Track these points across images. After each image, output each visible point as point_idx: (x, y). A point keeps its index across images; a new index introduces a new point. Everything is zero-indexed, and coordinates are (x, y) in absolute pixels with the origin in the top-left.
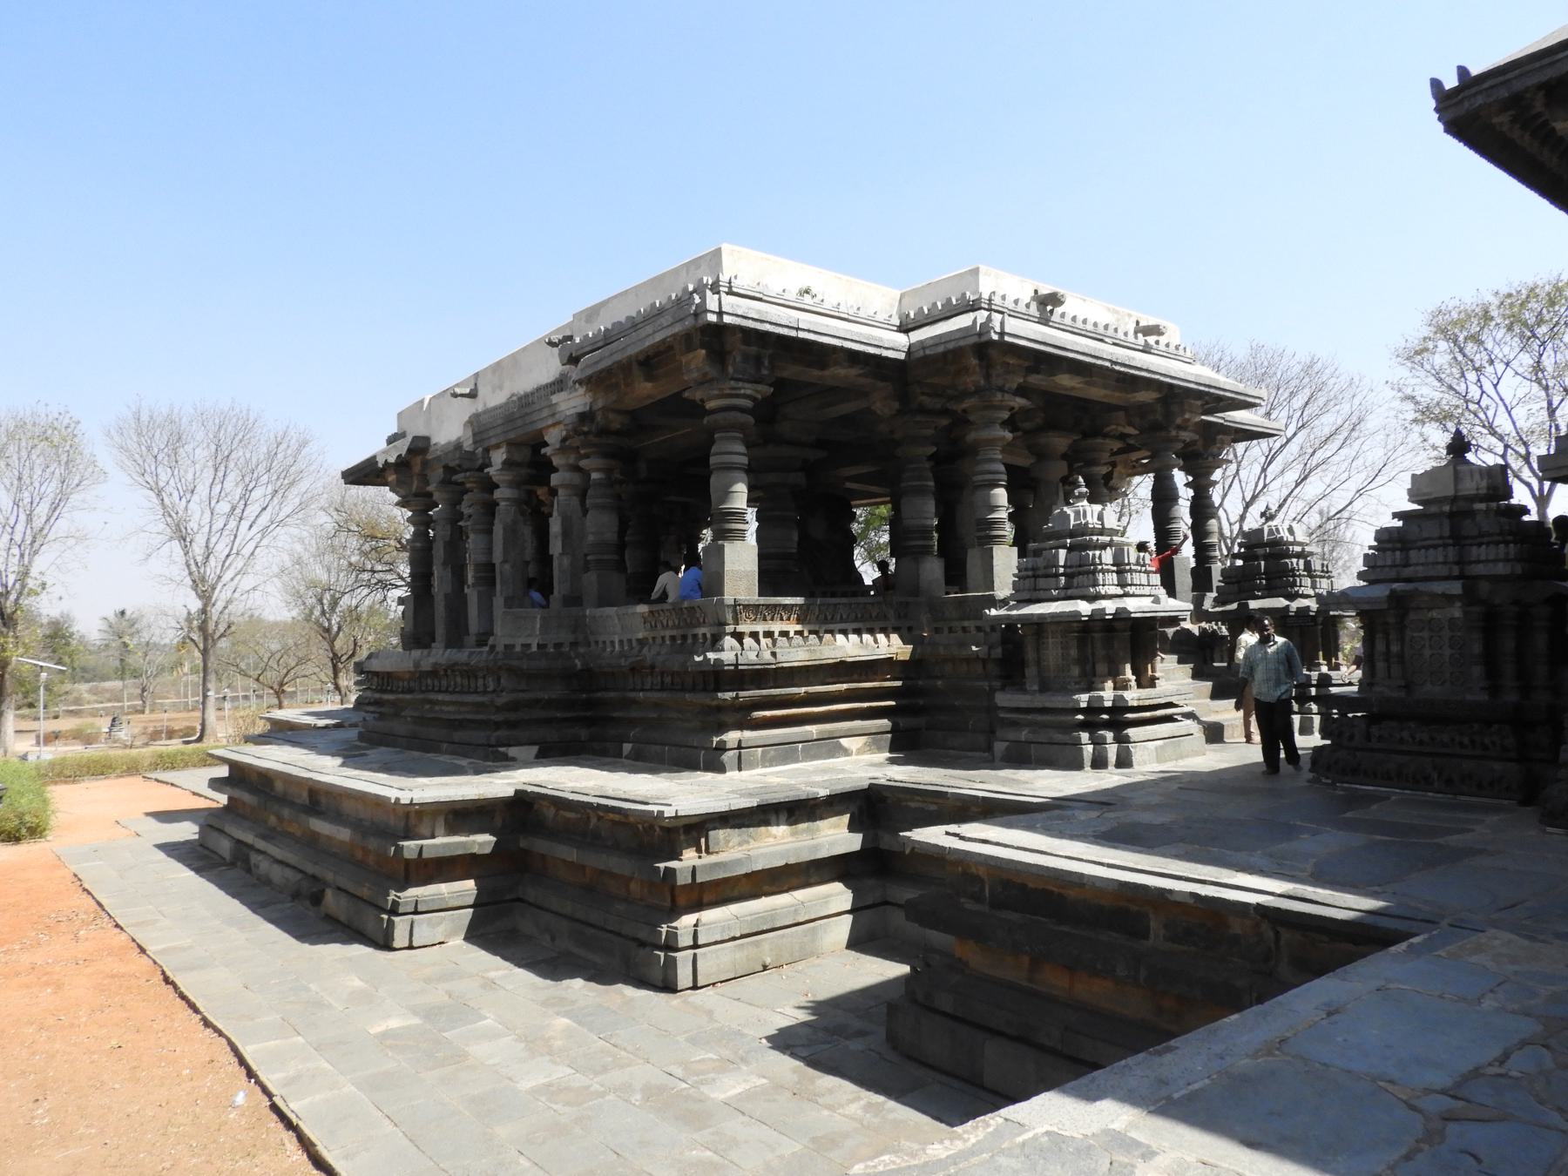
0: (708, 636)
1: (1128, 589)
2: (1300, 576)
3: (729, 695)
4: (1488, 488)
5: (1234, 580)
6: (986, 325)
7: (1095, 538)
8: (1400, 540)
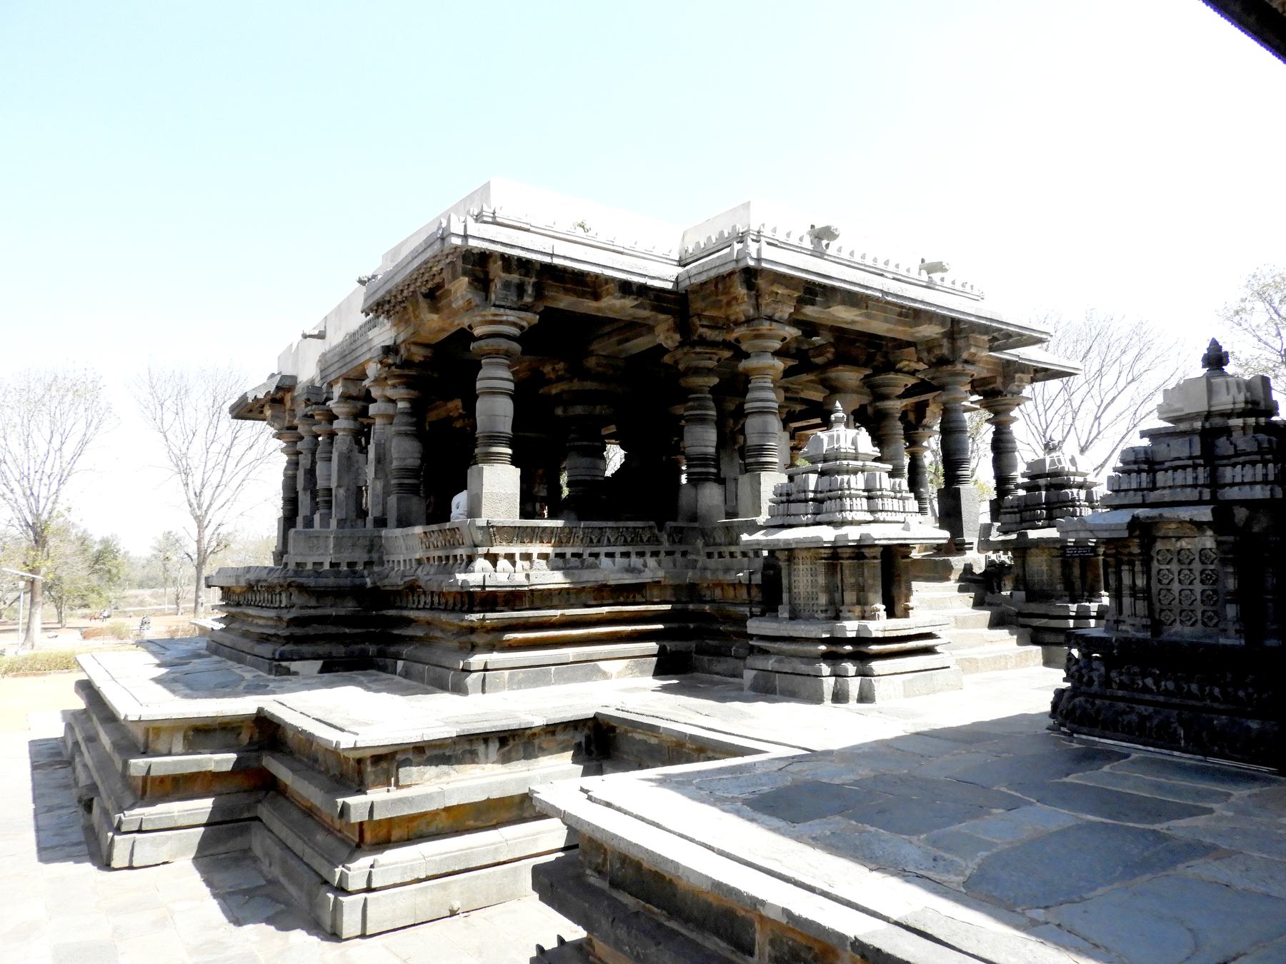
0: (464, 557)
1: (881, 516)
2: (1079, 506)
3: (475, 617)
4: (1246, 402)
5: (1016, 510)
6: (743, 254)
7: (845, 462)
8: (1147, 461)
